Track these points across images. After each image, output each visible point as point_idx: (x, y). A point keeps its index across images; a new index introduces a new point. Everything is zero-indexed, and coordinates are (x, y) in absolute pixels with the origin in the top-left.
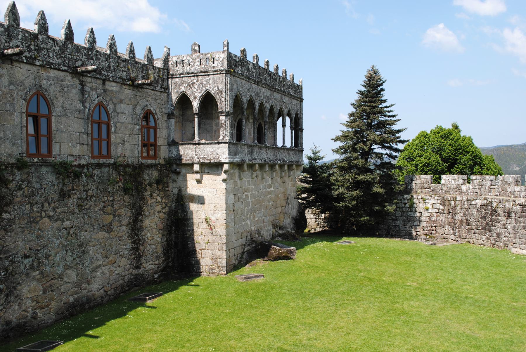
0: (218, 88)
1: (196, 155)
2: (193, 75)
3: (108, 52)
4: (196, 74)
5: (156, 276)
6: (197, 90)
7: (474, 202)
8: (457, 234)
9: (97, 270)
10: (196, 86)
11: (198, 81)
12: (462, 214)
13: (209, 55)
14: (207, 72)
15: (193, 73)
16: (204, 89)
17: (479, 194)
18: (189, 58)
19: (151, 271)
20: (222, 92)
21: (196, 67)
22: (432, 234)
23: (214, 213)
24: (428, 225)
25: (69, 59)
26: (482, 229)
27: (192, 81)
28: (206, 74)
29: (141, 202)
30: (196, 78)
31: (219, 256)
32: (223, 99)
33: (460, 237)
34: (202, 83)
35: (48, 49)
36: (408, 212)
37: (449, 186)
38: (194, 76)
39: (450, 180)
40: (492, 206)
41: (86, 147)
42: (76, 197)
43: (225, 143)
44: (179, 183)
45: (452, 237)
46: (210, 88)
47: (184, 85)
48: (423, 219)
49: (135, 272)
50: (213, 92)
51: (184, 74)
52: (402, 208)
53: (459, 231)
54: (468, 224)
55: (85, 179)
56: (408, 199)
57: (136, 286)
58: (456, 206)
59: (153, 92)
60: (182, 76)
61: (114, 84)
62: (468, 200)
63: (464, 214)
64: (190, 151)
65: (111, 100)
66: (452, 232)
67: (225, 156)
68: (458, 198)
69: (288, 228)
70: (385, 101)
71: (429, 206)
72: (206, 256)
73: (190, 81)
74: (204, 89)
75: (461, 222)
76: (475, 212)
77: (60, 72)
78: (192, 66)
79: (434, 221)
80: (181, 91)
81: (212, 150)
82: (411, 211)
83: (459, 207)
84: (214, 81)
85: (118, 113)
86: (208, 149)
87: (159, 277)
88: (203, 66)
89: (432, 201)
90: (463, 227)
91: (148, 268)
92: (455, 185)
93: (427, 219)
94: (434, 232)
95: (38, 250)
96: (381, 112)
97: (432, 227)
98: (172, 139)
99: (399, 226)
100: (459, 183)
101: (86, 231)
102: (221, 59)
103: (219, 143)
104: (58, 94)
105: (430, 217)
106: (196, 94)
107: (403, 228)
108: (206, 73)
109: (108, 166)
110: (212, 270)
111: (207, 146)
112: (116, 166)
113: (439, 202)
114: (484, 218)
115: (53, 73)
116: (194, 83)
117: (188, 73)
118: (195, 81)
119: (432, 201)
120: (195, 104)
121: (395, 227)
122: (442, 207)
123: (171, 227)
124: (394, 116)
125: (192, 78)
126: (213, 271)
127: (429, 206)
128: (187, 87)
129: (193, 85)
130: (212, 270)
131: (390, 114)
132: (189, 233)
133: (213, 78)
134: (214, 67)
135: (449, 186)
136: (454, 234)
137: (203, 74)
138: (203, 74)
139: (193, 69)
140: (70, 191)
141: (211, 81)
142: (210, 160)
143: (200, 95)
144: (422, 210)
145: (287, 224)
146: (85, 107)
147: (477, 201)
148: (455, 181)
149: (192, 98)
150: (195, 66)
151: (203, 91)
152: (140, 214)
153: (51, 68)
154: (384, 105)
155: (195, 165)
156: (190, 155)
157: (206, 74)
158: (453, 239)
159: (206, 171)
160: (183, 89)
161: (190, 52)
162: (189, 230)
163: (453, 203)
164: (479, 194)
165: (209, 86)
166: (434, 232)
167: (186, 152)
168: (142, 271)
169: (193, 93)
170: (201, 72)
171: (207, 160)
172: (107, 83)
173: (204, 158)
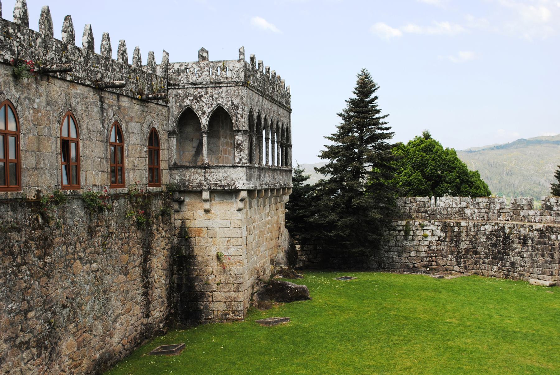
0: (233, 103)
1: (206, 181)
2: (201, 86)
3: (120, 61)
4: (204, 86)
5: (161, 325)
6: (206, 104)
7: (482, 228)
8: (462, 265)
9: (117, 320)
10: (204, 100)
11: (207, 93)
12: (467, 242)
13: (221, 64)
14: (219, 83)
15: (201, 83)
16: (215, 103)
17: (486, 218)
18: (194, 66)
19: (158, 320)
20: (237, 107)
21: (205, 77)
22: (431, 265)
23: (228, 248)
24: (426, 255)
25: (92, 71)
26: (493, 258)
28: (218, 85)
29: (150, 238)
30: (204, 90)
31: (235, 298)
32: (239, 116)
33: (465, 268)
34: (212, 96)
35: (75, 61)
36: (403, 241)
37: (449, 209)
38: (202, 88)
39: (451, 203)
40: (504, 233)
41: (105, 174)
42: (100, 234)
43: (242, 167)
44: (183, 214)
45: (456, 268)
46: (222, 102)
47: (189, 98)
48: (422, 248)
49: (145, 321)
51: (188, 84)
52: (396, 236)
53: (465, 261)
54: (476, 253)
55: (107, 212)
56: (403, 226)
57: (146, 338)
58: (460, 233)
59: (156, 106)
60: (186, 87)
61: (126, 99)
62: (475, 226)
63: (471, 242)
64: (197, 176)
65: (124, 118)
66: (456, 263)
67: (242, 182)
68: (463, 224)
69: (281, 264)
70: (378, 111)
71: (428, 233)
72: (218, 299)
73: (196, 93)
74: (215, 103)
75: (467, 251)
76: (483, 239)
77: (84, 87)
78: (199, 76)
80: (185, 104)
81: (225, 175)
82: (406, 240)
83: (464, 234)
85: (129, 133)
86: (221, 174)
87: (164, 327)
88: (214, 77)
89: (432, 227)
90: (469, 257)
91: (155, 316)
92: (457, 209)
93: (426, 248)
94: (434, 263)
95: (73, 299)
97: (431, 257)
98: (173, 161)
99: (392, 257)
100: (461, 206)
101: (109, 274)
102: (236, 69)
103: (234, 167)
104: (84, 113)
105: (429, 247)
106: (205, 109)
107: (398, 260)
108: (217, 84)
109: (124, 196)
110: (226, 315)
111: (220, 170)
112: (129, 196)
113: (439, 228)
114: (494, 245)
115: (80, 89)
116: (202, 96)
117: (194, 84)
118: (203, 93)
119: (432, 227)
120: (204, 121)
121: (388, 258)
122: (443, 235)
123: (173, 267)
124: (387, 129)
125: (199, 90)
126: (227, 316)
127: (428, 233)
128: (193, 100)
129: (200, 98)
130: (226, 315)
131: (384, 126)
132: (196, 273)
133: (227, 91)
134: (227, 78)
135: (449, 209)
136: (458, 264)
137: (213, 85)
138: (213, 85)
139: (200, 79)
140: (95, 227)
141: (224, 95)
142: (224, 186)
143: (209, 110)
145: (280, 259)
146: (104, 127)
147: (486, 227)
148: (456, 204)
149: (199, 113)
150: (204, 76)
151: (213, 106)
152: (148, 253)
153: (78, 83)
154: (377, 115)
156: (198, 181)
157: (218, 85)
158: (458, 270)
159: (217, 199)
160: (187, 102)
161: (197, 59)
162: (196, 270)
163: (456, 229)
164: (486, 218)
165: (221, 99)
166: (434, 263)
167: (192, 178)
168: (150, 320)
169: (201, 107)
170: (212, 83)
171: (220, 186)
172: (121, 98)
173: (215, 185)
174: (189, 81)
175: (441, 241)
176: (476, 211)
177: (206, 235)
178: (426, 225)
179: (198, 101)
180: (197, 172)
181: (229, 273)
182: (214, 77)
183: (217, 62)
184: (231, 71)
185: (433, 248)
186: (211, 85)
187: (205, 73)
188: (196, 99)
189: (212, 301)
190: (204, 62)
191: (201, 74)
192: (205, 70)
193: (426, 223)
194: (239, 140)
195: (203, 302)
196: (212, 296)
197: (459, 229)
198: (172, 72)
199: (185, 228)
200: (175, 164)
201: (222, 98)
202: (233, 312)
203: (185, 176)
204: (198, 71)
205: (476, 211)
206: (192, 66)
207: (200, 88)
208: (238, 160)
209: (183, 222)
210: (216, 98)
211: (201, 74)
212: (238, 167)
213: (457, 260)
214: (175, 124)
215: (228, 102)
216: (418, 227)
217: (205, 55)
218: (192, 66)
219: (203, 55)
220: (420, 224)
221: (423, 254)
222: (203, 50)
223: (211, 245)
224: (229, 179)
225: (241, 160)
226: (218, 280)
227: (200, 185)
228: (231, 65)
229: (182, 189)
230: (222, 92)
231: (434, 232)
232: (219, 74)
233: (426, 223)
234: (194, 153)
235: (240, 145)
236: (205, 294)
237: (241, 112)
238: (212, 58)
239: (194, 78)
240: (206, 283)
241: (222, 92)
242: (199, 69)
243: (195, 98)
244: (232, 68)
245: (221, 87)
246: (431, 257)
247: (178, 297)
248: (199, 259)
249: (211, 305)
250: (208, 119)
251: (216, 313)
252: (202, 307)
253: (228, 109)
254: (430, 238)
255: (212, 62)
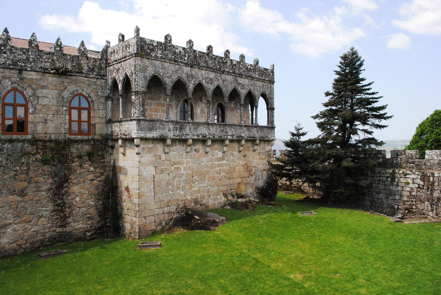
14: (125, 57)
19: (82, 230)
22: (412, 208)
24: (408, 199)
28: (125, 59)
29: (66, 172)
36: (390, 186)
43: (135, 120)
44: (114, 155)
48: (404, 193)
52: (385, 181)
56: (390, 174)
57: (59, 242)
59: (86, 79)
61: (33, 73)
69: (250, 197)
70: (363, 80)
71: (410, 181)
79: (413, 196)
81: (128, 127)
82: (392, 185)
85: (38, 97)
87: (91, 235)
91: (77, 227)
93: (408, 194)
94: (414, 207)
96: (361, 90)
97: (412, 201)
98: (108, 118)
99: (381, 198)
103: (131, 120)
105: (410, 192)
107: (385, 201)
112: (34, 142)
117: (116, 61)
121: (378, 199)
123: (109, 193)
124: (373, 94)
127: (410, 181)
131: (368, 92)
139: (119, 56)
144: (403, 185)
145: (249, 193)
152: (67, 181)
154: (363, 83)
157: (125, 59)
166: (414, 207)
168: (68, 229)
178: (408, 174)
185: (414, 193)
186: (123, 60)
193: (408, 172)
216: (402, 175)
220: (403, 173)
221: (405, 199)
231: (414, 180)
233: (408, 172)
237: (134, 77)
254: (411, 185)
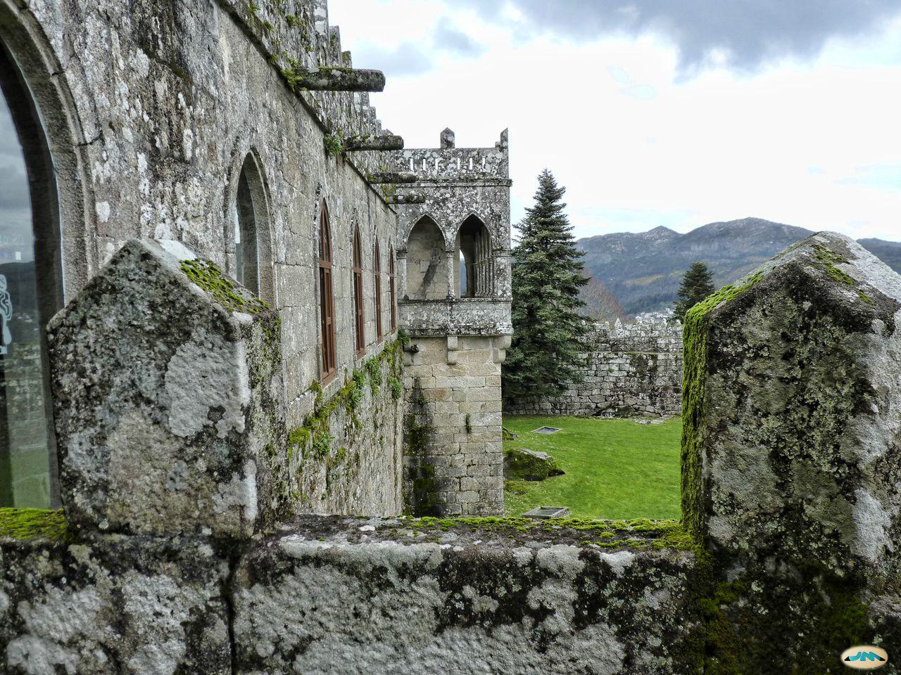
1: (453, 322)
2: (445, 185)
4: (450, 184)
6: (453, 212)
8: (658, 405)
10: (450, 205)
11: (453, 196)
12: (666, 379)
13: (475, 153)
14: (473, 181)
15: (445, 181)
16: (465, 209)
18: (435, 154)
20: (500, 216)
23: (482, 416)
24: (612, 393)
27: (442, 195)
31: (492, 485)
32: (502, 229)
33: (663, 408)
34: (461, 200)
37: (636, 339)
38: (446, 187)
43: (506, 301)
45: (650, 408)
46: (477, 209)
48: (605, 385)
50: (482, 217)
51: (425, 181)
53: (662, 401)
58: (654, 369)
63: (670, 378)
64: (439, 315)
71: (615, 368)
73: (438, 194)
74: (465, 209)
75: (666, 388)
80: (421, 210)
81: (482, 313)
83: (661, 369)
84: (485, 198)
86: (475, 312)
88: (464, 171)
90: (668, 396)
94: (621, 403)
100: (653, 335)
102: (498, 161)
106: (450, 219)
110: (479, 508)
113: (628, 361)
116: (447, 199)
117: (435, 181)
118: (448, 196)
120: (450, 235)
122: (634, 369)
125: (442, 190)
126: (481, 510)
127: (615, 368)
128: (433, 204)
129: (444, 203)
130: (479, 508)
132: (436, 452)
133: (483, 193)
134: (484, 174)
136: (653, 404)
137: (464, 184)
138: (464, 184)
139: (443, 174)
141: (478, 198)
142: (480, 329)
143: (457, 220)
144: (604, 374)
148: (646, 332)
151: (464, 214)
155: (449, 339)
156: (441, 322)
158: (652, 411)
160: (424, 208)
161: (438, 145)
163: (651, 363)
167: (432, 317)
169: (445, 216)
173: (468, 328)
174: (427, 177)
175: (631, 376)
176: (673, 341)
177: (451, 399)
179: (440, 206)
180: (439, 309)
181: (483, 451)
182: (464, 171)
183: (469, 151)
184: (490, 164)
186: (460, 184)
187: (451, 166)
188: (438, 204)
189: (460, 490)
190: (449, 150)
191: (446, 167)
192: (451, 161)
193: (612, 355)
194: (502, 264)
195: (447, 492)
196: (460, 483)
197: (655, 363)
198: (401, 163)
199: (420, 389)
200: (406, 298)
201: (477, 203)
202: (490, 504)
203: (420, 314)
204: (441, 162)
205: (673, 341)
206: (432, 155)
207: (444, 187)
208: (500, 293)
209: (416, 380)
210: (468, 203)
211: (446, 167)
212: (500, 301)
213: (651, 398)
214: (405, 240)
215: (485, 208)
216: (603, 360)
217: (450, 139)
218: (432, 155)
219: (447, 139)
220: (604, 357)
221: (608, 393)
222: (447, 132)
223: (458, 412)
224: (486, 319)
225: (504, 292)
226: (468, 460)
227: (444, 328)
228: (490, 155)
229: (417, 333)
230: (476, 194)
232: (471, 168)
234: (421, 280)
235: (504, 271)
236: (449, 481)
238: (459, 143)
239: (435, 173)
240: (451, 466)
241: (476, 194)
242: (441, 159)
243: (436, 202)
244: (490, 160)
245: (474, 187)
246: (618, 395)
247: (410, 487)
248: (441, 432)
249: (459, 496)
250: (456, 233)
251: (465, 506)
252: (445, 499)
253: (485, 219)
254: (616, 374)
255: (462, 150)
